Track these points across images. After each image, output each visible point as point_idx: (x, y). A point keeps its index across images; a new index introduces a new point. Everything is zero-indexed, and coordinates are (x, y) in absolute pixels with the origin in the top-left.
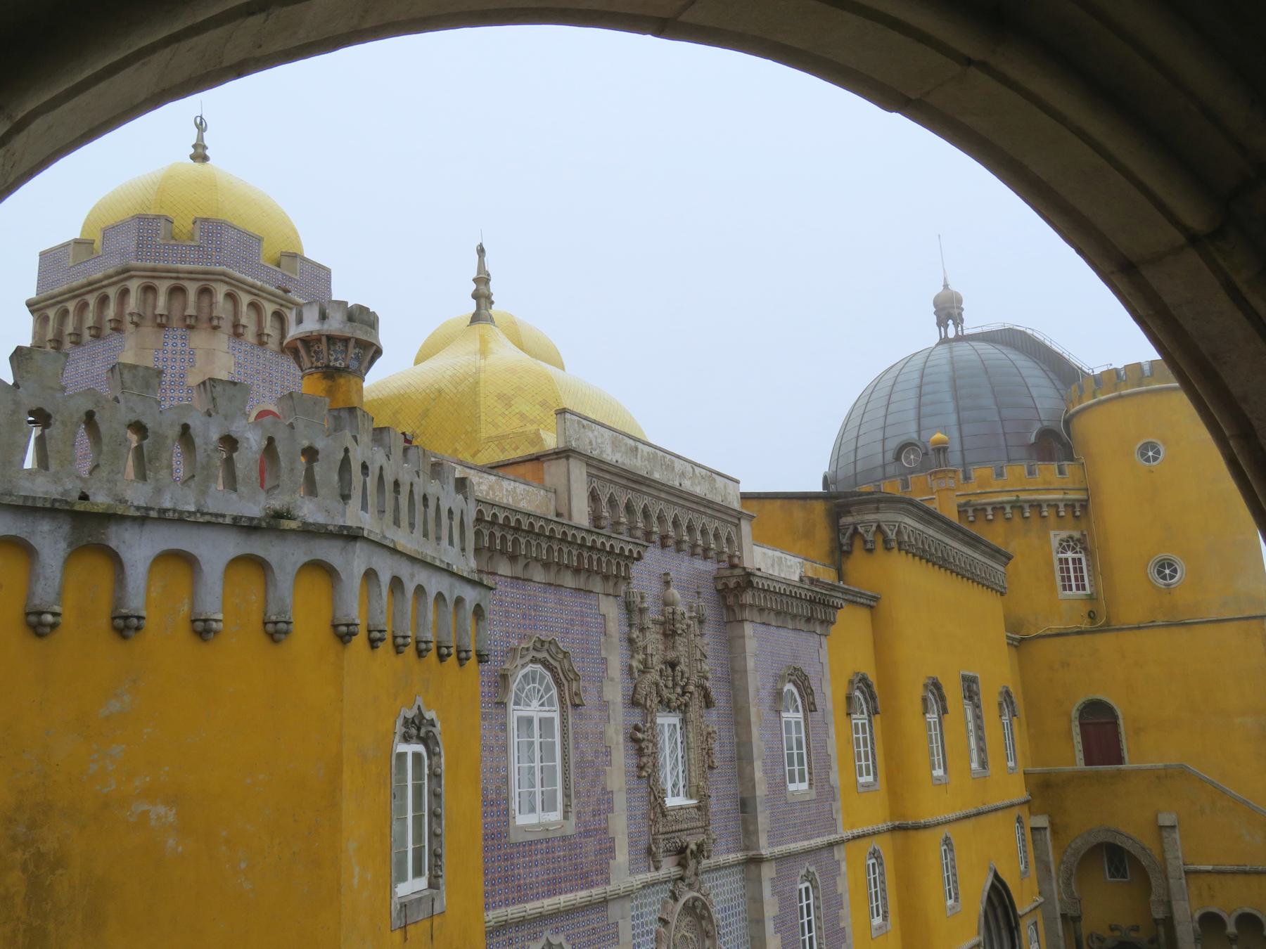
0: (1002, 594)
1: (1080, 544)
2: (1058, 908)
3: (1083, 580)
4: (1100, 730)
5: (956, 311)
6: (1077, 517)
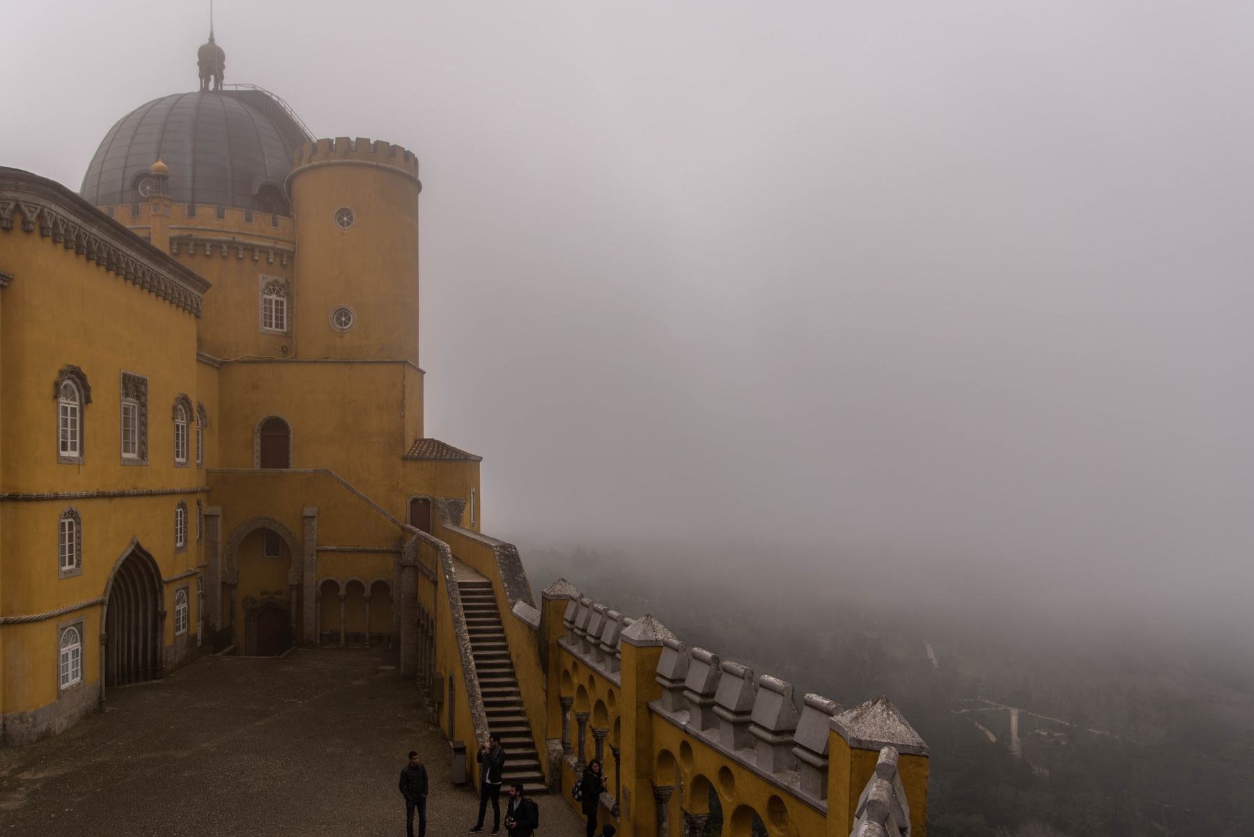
2: (220, 577)
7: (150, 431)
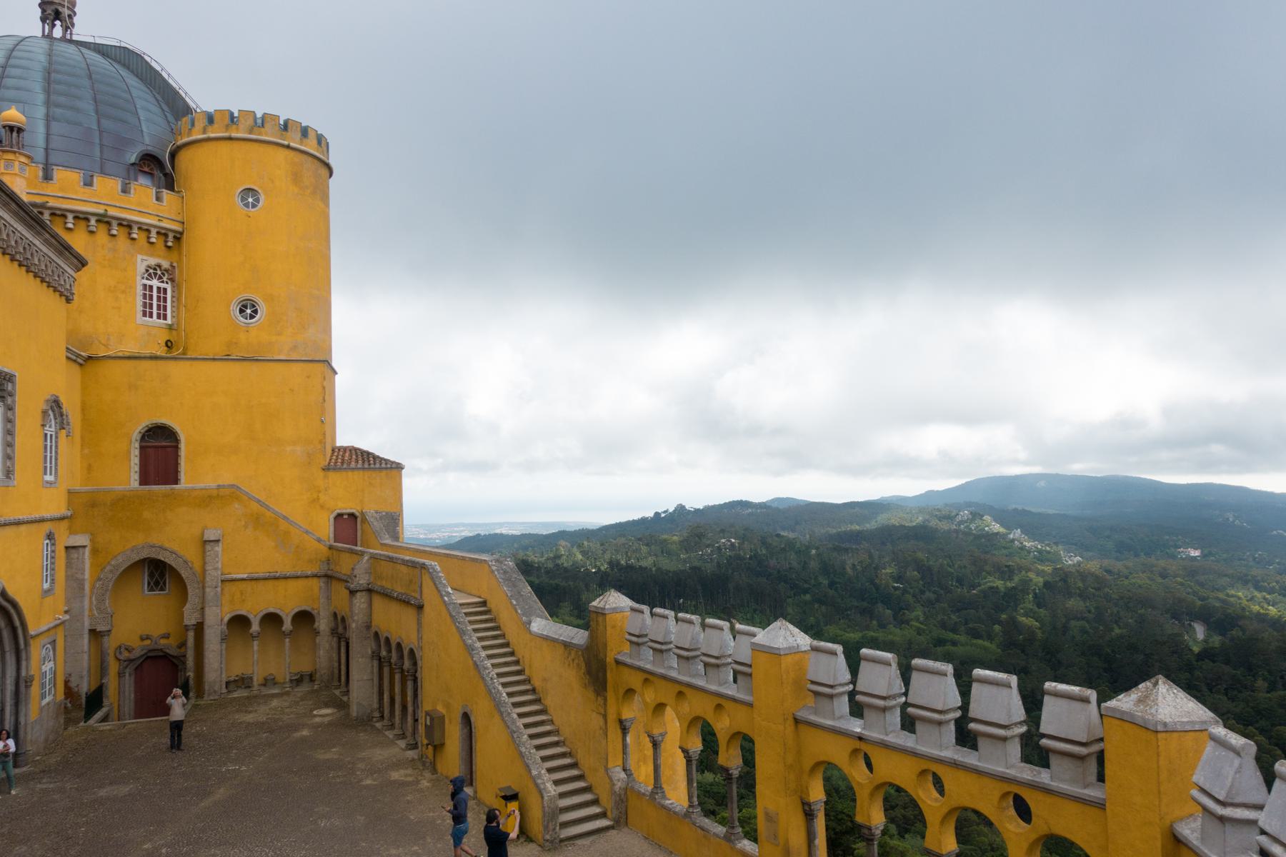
0: (68, 300)
1: (168, 274)
3: (165, 309)
4: (160, 451)
5: (66, 12)
6: (169, 247)
7: (19, 440)
